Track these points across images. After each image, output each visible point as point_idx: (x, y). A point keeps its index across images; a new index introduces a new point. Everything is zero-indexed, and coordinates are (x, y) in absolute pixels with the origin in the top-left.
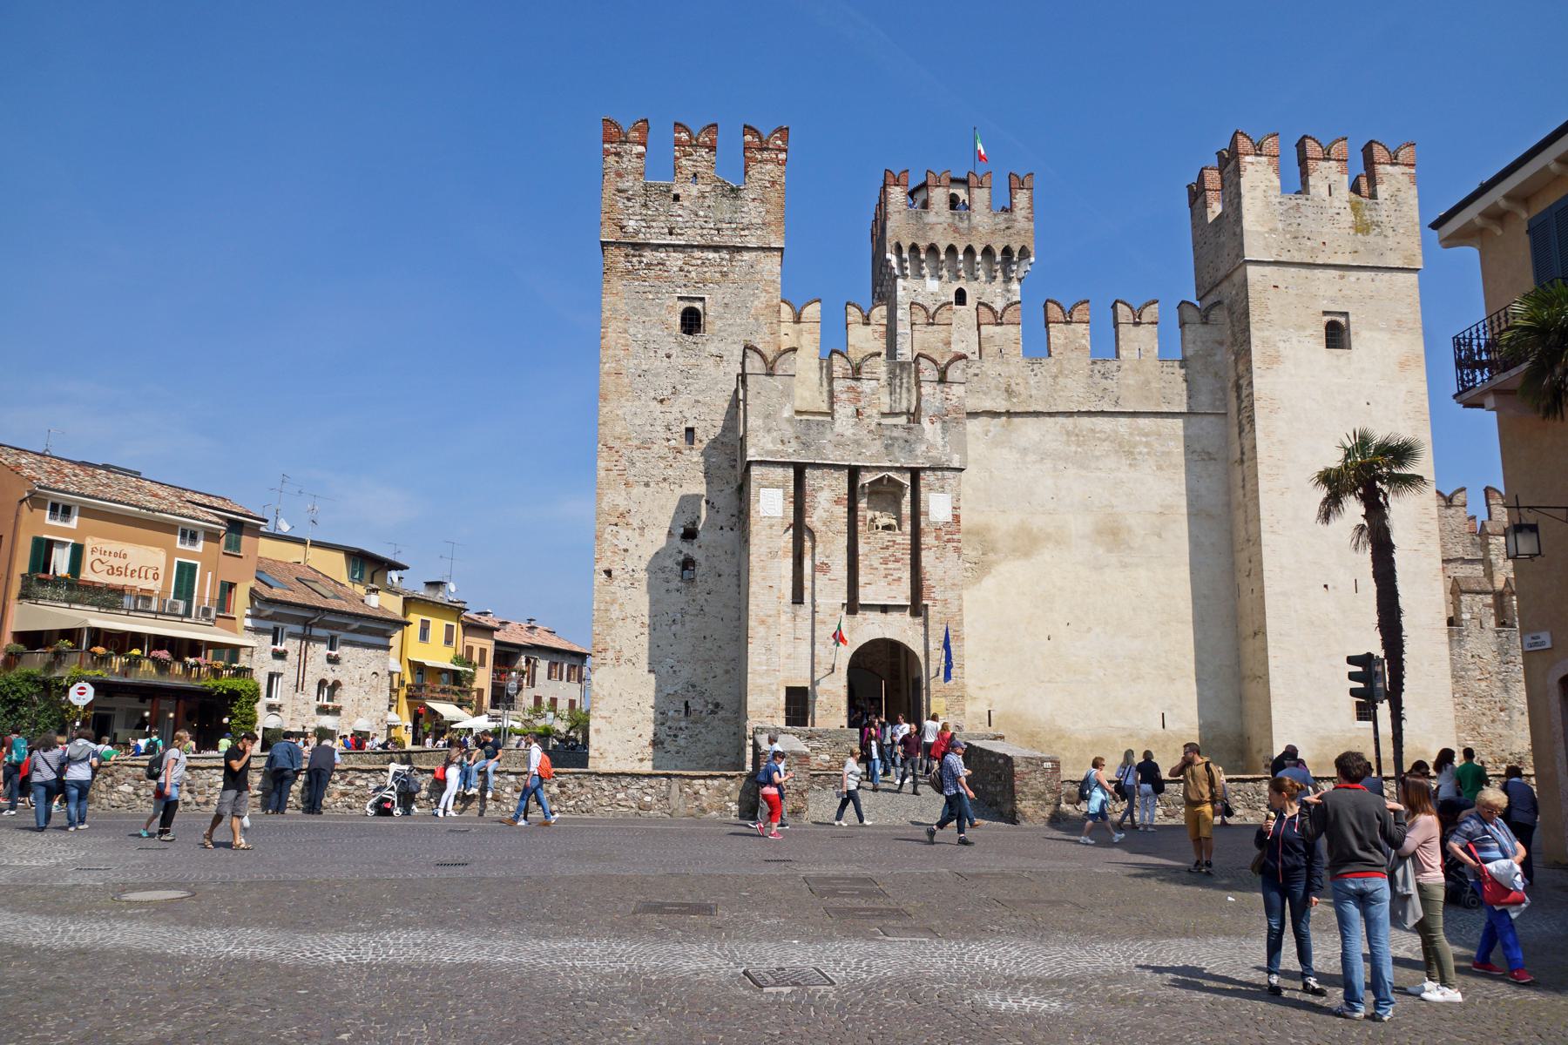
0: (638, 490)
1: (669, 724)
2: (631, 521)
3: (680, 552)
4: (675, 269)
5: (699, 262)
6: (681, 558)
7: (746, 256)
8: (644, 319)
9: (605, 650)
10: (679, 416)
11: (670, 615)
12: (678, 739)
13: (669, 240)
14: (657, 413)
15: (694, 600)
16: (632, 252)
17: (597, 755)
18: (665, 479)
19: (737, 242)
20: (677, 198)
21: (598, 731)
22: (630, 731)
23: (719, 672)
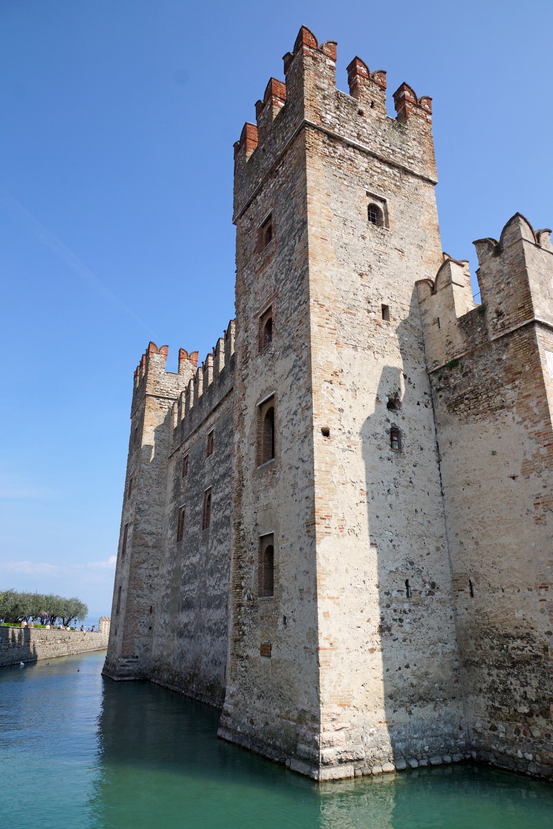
0: (348, 352)
1: (394, 606)
2: (344, 381)
3: (388, 421)
4: (364, 169)
5: (379, 171)
6: (389, 426)
7: (412, 180)
8: (342, 199)
9: (329, 517)
10: (375, 291)
11: (386, 483)
12: (403, 624)
13: (357, 142)
14: (358, 285)
15: (403, 471)
16: (328, 141)
17: (327, 646)
18: (369, 348)
19: (406, 165)
20: (361, 113)
21: (326, 615)
22: (359, 615)
23: (432, 549)
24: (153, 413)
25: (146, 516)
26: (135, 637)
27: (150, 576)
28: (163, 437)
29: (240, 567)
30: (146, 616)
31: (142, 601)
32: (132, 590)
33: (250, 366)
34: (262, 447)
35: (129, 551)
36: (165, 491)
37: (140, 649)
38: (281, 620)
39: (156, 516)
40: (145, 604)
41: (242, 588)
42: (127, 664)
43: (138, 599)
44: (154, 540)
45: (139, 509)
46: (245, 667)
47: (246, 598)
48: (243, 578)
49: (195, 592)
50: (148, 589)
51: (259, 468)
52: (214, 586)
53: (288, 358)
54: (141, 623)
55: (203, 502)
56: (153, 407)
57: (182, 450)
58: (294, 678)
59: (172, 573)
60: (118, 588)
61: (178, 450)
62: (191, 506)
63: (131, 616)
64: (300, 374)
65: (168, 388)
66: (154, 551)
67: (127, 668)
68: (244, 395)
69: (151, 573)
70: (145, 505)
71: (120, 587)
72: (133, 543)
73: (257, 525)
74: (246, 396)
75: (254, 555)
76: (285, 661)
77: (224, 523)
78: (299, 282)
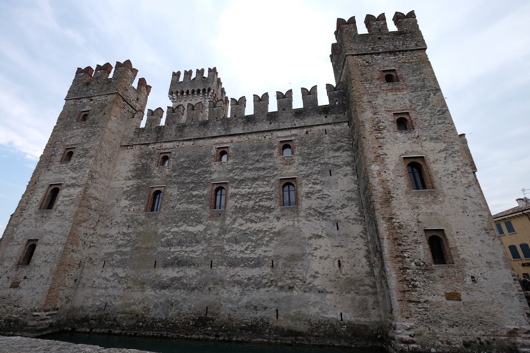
24: (118, 109)
26: (61, 290)
27: (86, 234)
28: (120, 129)
29: (400, 245)
30: (75, 269)
31: (74, 255)
32: (69, 245)
36: (112, 169)
38: (468, 280)
39: (102, 186)
40: (77, 259)
42: (47, 317)
43: (72, 253)
44: (97, 204)
45: (92, 176)
47: (413, 264)
49: (196, 253)
50: (82, 245)
53: (439, 144)
58: (495, 312)
63: (62, 270)
64: (453, 155)
66: (94, 213)
67: (47, 322)
76: (481, 302)
78: (441, 113)
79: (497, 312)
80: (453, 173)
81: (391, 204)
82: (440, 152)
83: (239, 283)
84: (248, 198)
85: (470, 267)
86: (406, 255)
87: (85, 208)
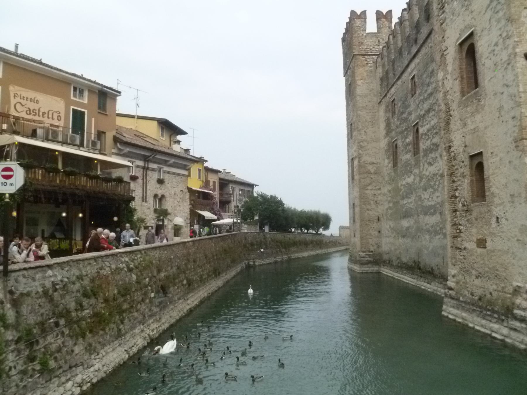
25: (366, 150)
27: (375, 195)
28: (371, 87)
29: (454, 181)
31: (370, 212)
32: (363, 206)
33: (447, 11)
34: (465, 81)
35: (357, 177)
37: (373, 246)
38: (494, 220)
41: (456, 197)
43: (368, 212)
45: (361, 146)
46: (464, 256)
47: (460, 205)
48: (456, 190)
49: (413, 204)
51: (464, 98)
52: (428, 199)
54: (372, 228)
55: (412, 134)
56: (361, 64)
57: (389, 95)
58: (508, 263)
59: (392, 192)
60: (352, 205)
61: (386, 95)
62: (402, 139)
63: (365, 224)
65: (371, 46)
66: (376, 176)
68: (443, 37)
69: (376, 192)
70: (364, 142)
71: (354, 204)
72: (360, 172)
73: (466, 146)
74: (445, 38)
75: (467, 171)
76: (499, 250)
77: (432, 149)
79: (510, 265)
80: (495, 47)
81: (449, 126)
82: (486, 11)
83: (428, 231)
84: (427, 137)
85: (497, 204)
86: (457, 194)
87: (365, 175)
